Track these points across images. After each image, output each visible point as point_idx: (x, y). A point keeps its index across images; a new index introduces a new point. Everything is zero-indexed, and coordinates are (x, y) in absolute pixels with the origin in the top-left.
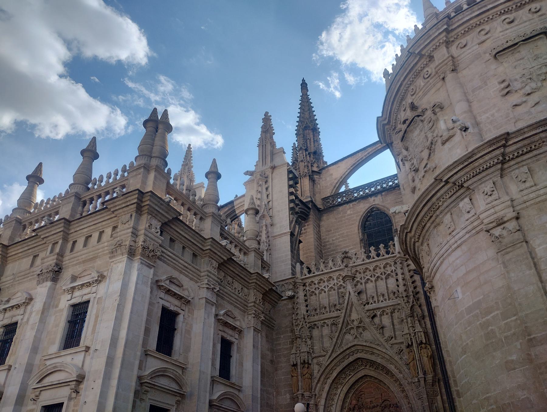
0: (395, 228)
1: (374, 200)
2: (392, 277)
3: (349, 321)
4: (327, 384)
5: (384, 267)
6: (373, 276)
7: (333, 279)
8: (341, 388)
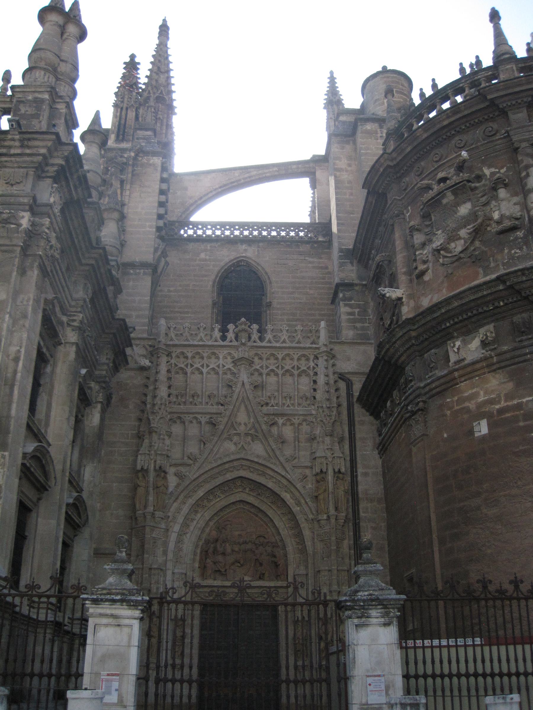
0: (268, 301)
1: (246, 250)
2: (308, 375)
3: (234, 423)
4: (187, 505)
5: (299, 359)
6: (280, 367)
7: (218, 358)
8: (202, 513)
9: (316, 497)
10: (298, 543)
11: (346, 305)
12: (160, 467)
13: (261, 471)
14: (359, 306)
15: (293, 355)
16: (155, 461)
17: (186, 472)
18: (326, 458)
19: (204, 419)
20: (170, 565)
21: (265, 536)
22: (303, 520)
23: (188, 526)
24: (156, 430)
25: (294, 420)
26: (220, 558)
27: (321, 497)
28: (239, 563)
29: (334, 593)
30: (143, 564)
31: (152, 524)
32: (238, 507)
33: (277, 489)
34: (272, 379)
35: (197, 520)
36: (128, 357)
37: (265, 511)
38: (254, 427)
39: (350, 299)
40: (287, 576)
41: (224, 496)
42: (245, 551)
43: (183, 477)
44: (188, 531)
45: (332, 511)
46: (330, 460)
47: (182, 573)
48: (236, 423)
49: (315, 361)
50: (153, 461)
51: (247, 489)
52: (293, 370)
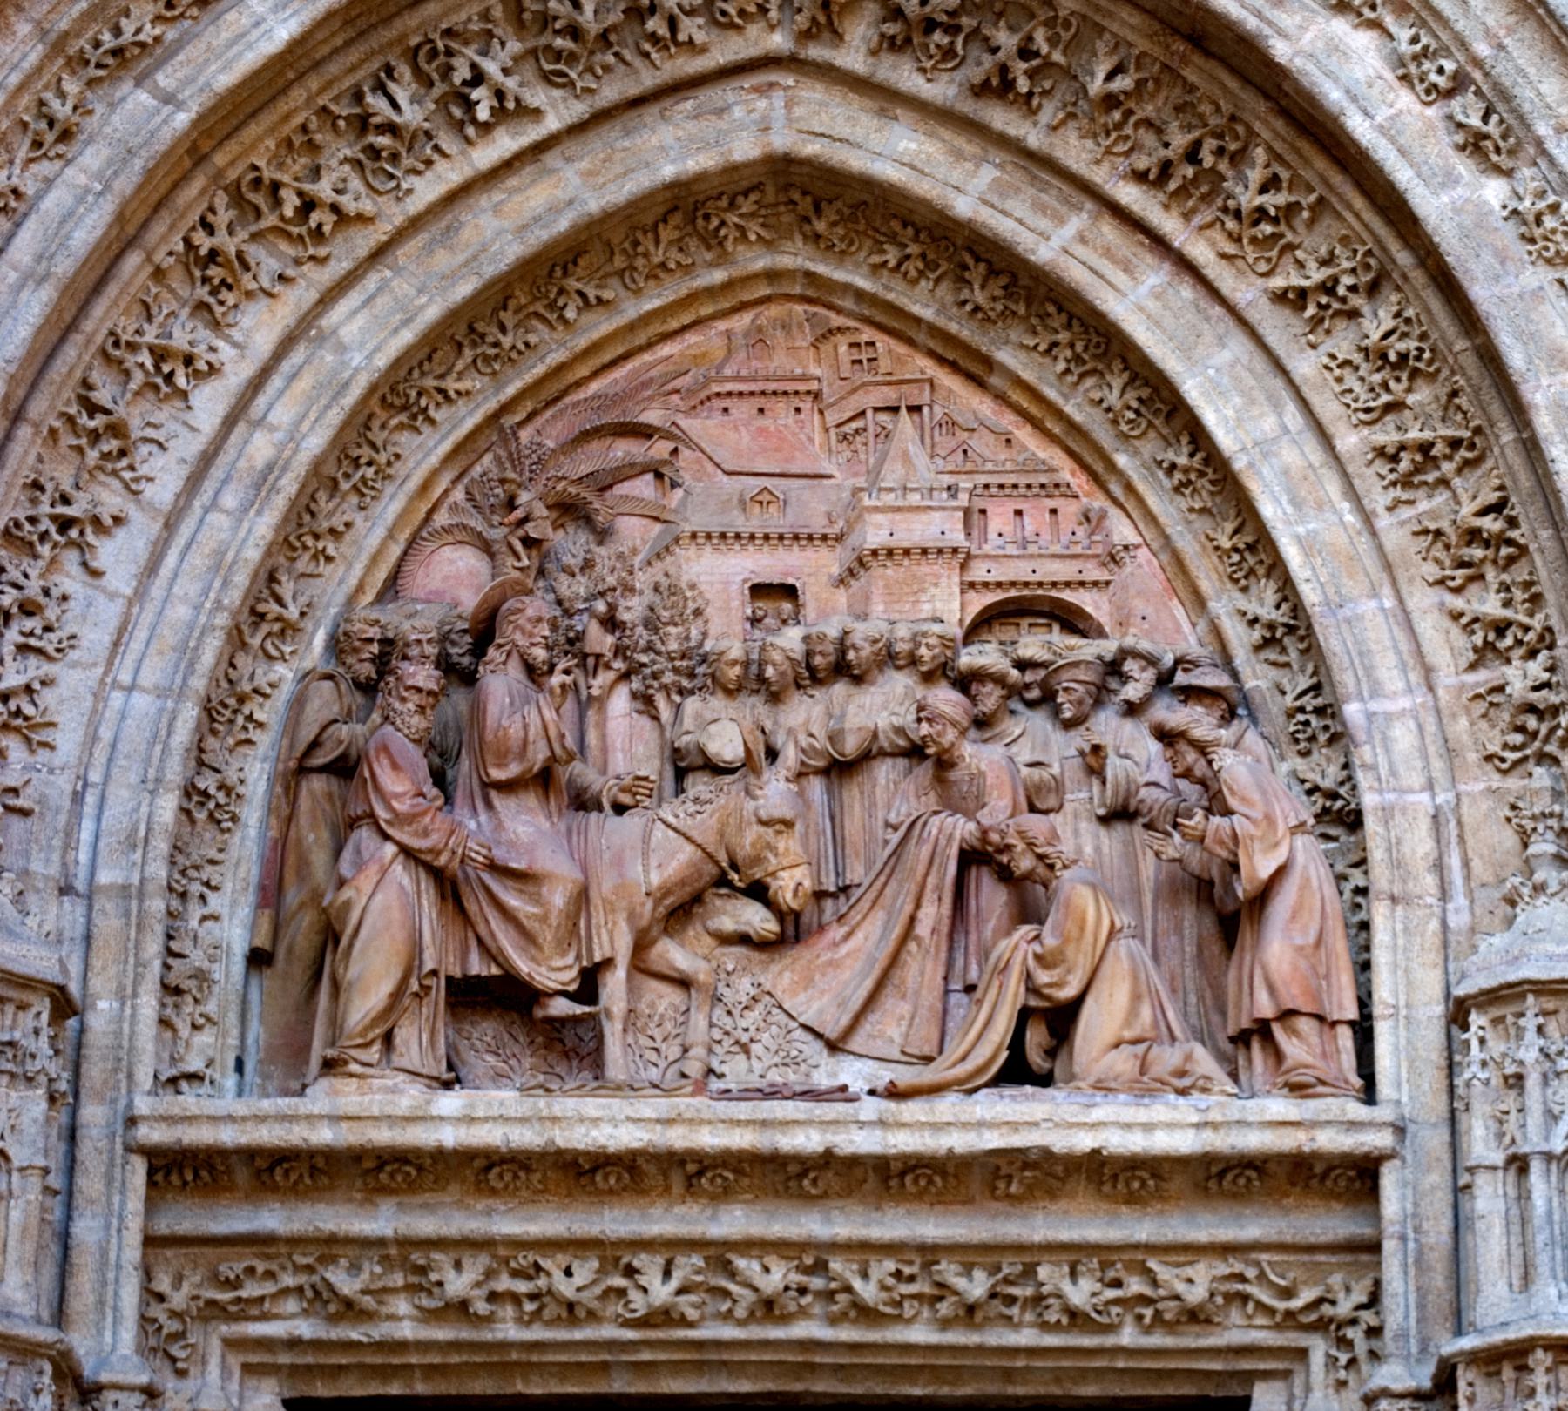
4: (91, 158)
8: (297, 298)
21: (1085, 600)
28: (758, 892)
32: (761, 262)
35: (237, 373)
37: (1076, 275)
40: (1363, 1032)
41: (579, 110)
44: (110, 498)
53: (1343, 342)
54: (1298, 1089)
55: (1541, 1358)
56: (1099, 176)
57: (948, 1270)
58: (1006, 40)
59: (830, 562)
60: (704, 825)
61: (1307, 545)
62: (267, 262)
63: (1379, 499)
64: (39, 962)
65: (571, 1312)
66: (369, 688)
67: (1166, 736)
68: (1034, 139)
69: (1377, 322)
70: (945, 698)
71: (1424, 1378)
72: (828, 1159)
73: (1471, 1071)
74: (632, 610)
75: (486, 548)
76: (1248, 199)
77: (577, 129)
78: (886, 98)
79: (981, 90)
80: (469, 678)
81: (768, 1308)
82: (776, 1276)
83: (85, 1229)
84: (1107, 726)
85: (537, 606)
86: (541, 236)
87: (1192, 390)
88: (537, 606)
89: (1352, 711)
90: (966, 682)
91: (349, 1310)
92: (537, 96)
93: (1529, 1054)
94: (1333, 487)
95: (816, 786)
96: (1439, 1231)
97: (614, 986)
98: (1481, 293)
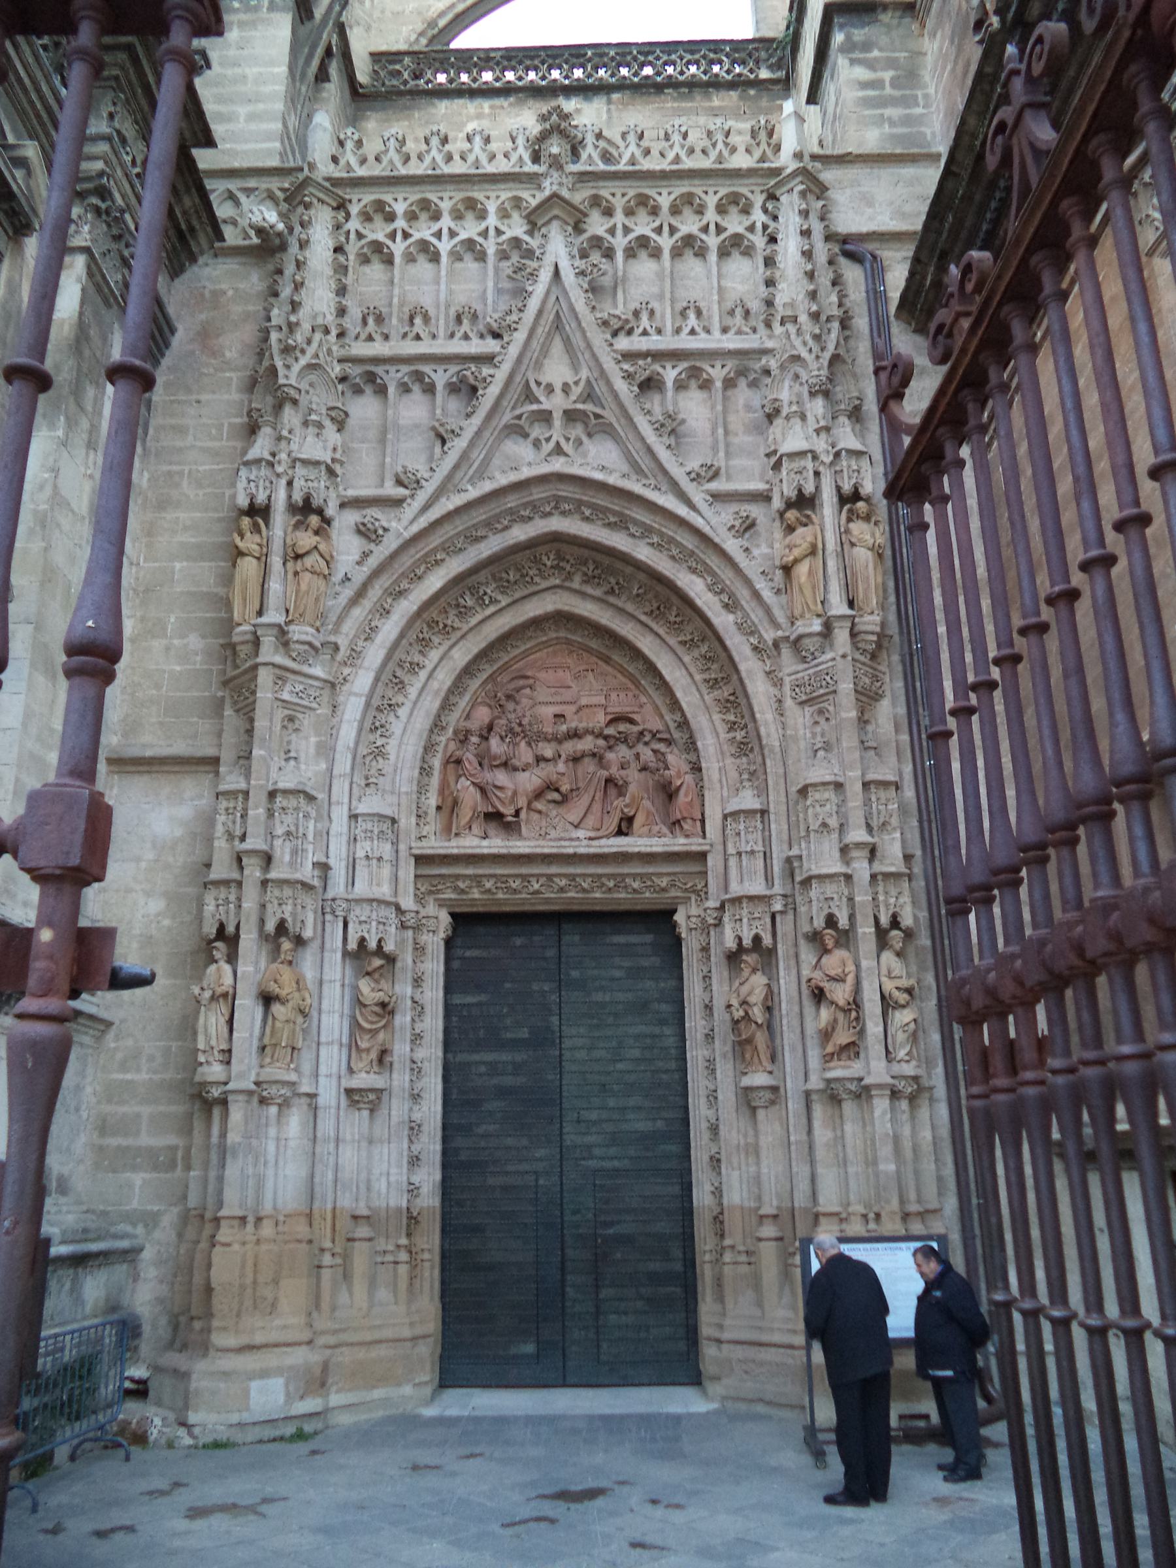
2: (748, 252)
6: (666, 229)
8: (442, 649)
9: (787, 569)
10: (732, 726)
11: (853, 62)
12: (307, 500)
13: (615, 513)
14: (891, 63)
15: (703, 196)
16: (290, 483)
17: (389, 521)
18: (815, 457)
19: (441, 377)
20: (340, 789)
21: (635, 716)
22: (748, 651)
23: (401, 686)
24: (292, 392)
25: (710, 370)
26: (501, 777)
27: (802, 570)
28: (557, 790)
29: (855, 853)
30: (248, 776)
31: (279, 659)
32: (553, 635)
33: (663, 564)
34: (644, 267)
35: (430, 666)
36: (223, 227)
37: (630, 637)
38: (589, 396)
39: (867, 46)
40: (703, 821)
41: (509, 600)
42: (576, 759)
43: (380, 532)
44: (400, 699)
45: (838, 606)
46: (828, 459)
47: (381, 817)
48: (538, 384)
49: (770, 206)
50: (283, 482)
51: (577, 578)
52: (704, 237)
53: (696, 653)
54: (687, 836)
55: (745, 901)
56: (636, 613)
57: (604, 880)
58: (613, 581)
59: (573, 708)
60: (543, 774)
61: (688, 703)
62: (436, 640)
63: (704, 691)
64: (388, 812)
65: (515, 891)
66: (461, 742)
67: (655, 751)
68: (620, 604)
69: (704, 649)
70: (601, 742)
71: (718, 905)
72: (575, 855)
73: (728, 832)
74: (525, 721)
75: (490, 706)
76: (672, 619)
77: (509, 605)
78: (583, 595)
79: (607, 593)
80: (487, 739)
81: (562, 890)
82: (563, 882)
83: (401, 874)
84: (640, 748)
85: (503, 722)
86: (502, 631)
87: (660, 665)
88: (503, 722)
89: (699, 744)
90: (606, 738)
91: (463, 891)
92: (499, 597)
93: (742, 827)
94: (694, 689)
95: (571, 764)
96: (721, 870)
97: (523, 815)
98: (728, 643)
